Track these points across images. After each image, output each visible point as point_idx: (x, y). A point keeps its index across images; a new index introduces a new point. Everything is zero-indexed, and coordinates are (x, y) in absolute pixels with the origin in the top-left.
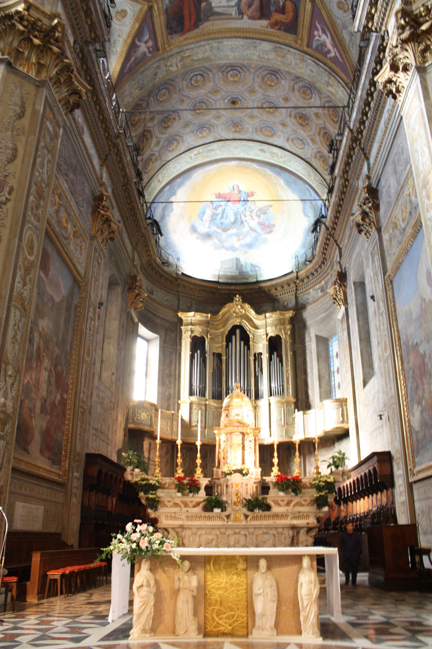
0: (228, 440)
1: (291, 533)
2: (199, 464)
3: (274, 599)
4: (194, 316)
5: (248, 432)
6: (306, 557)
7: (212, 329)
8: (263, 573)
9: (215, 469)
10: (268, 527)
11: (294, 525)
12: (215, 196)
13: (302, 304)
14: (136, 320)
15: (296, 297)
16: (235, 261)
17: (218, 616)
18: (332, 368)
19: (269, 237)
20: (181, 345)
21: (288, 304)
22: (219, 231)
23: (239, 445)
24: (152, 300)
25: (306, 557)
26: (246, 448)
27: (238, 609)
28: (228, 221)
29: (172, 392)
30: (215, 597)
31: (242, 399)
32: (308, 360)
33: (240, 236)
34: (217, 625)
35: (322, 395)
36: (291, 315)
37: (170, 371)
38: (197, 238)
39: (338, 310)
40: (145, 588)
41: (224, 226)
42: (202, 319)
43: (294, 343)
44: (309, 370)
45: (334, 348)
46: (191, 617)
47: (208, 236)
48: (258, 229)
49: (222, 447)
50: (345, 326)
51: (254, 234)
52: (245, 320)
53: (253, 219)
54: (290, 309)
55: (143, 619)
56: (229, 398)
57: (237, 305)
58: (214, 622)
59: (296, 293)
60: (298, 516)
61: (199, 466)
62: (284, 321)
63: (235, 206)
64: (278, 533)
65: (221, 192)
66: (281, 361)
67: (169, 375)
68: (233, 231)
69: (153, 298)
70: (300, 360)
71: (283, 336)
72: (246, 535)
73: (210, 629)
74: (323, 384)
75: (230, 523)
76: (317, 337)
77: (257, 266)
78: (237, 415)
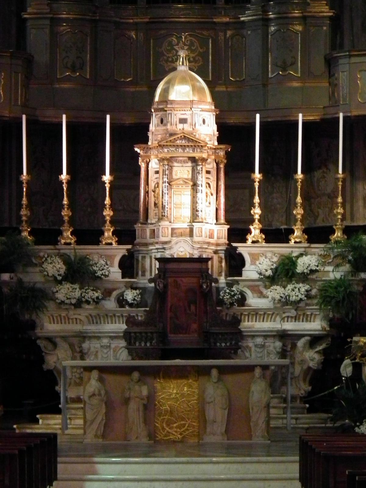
1: (278, 344)
3: (225, 407)
6: (258, 367)
8: (215, 383)
9: (138, 227)
11: (285, 331)
17: (168, 425)
25: (258, 367)
27: (189, 419)
30: (165, 408)
34: (167, 434)
40: (97, 397)
46: (142, 425)
49: (152, 185)
58: (164, 432)
61: (108, 222)
64: (256, 346)
73: (160, 437)
78: (183, 121)
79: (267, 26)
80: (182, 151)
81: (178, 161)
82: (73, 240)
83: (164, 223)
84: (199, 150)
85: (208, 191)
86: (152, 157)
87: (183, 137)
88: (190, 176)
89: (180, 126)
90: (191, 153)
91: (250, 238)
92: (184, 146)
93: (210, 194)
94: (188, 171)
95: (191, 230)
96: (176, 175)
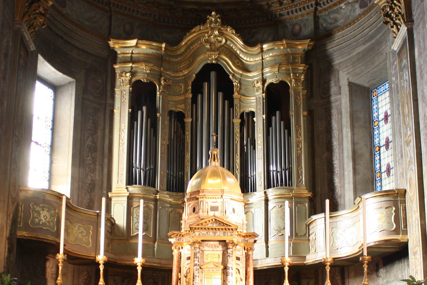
0: (195, 254)
4: (136, 46)
5: (235, 241)
7: (167, 70)
13: (325, 29)
14: (32, 47)
15: (316, 18)
18: (376, 141)
20: (113, 97)
21: (301, 29)
24: (63, 15)
26: (230, 271)
29: (97, 178)
31: (224, 179)
32: (335, 125)
35: (359, 187)
36: (306, 47)
37: (93, 142)
39: (391, 35)
42: (151, 51)
43: (309, 97)
44: (335, 143)
45: (380, 105)
49: (184, 271)
50: (406, 62)
52: (226, 55)
54: (305, 38)
56: (197, 178)
57: (213, 29)
59: (316, 9)
62: (294, 58)
66: (288, 127)
67: (93, 149)
69: (64, 12)
70: (320, 126)
71: (292, 84)
74: (361, 168)
76: (351, 85)
78: (215, 209)
80: (213, 235)
81: (209, 245)
84: (229, 234)
85: (238, 276)
86: (184, 244)
87: (214, 220)
88: (221, 260)
89: (211, 213)
90: (222, 236)
92: (215, 229)
93: (240, 280)
94: (219, 255)
96: (207, 259)
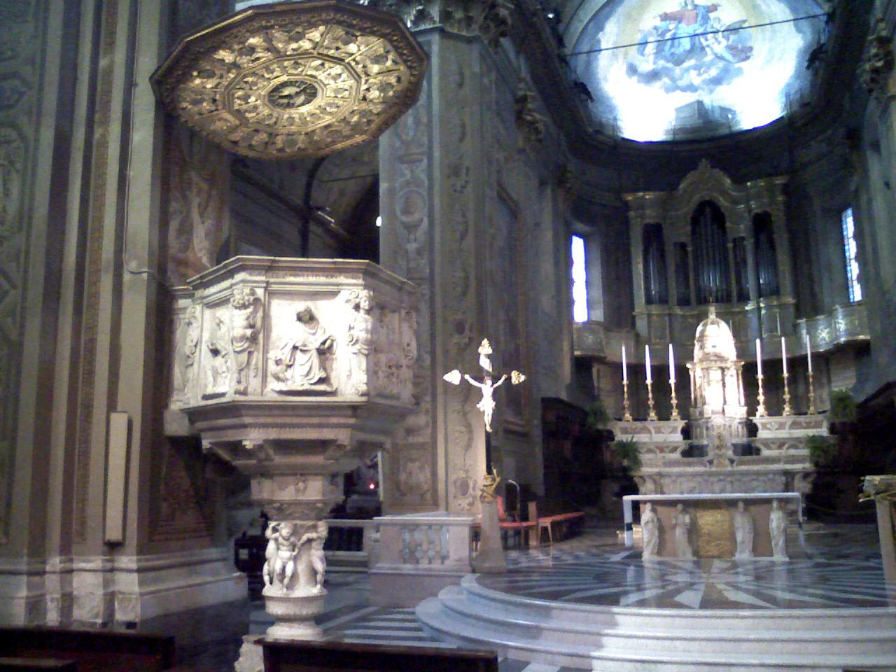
1: (783, 478)
2: (674, 405)
5: (729, 366)
9: (691, 410)
10: (758, 473)
12: (659, 19)
16: (696, 106)
19: (743, 65)
22: (670, 65)
23: (718, 382)
28: (682, 50)
33: (700, 69)
38: (639, 81)
40: (650, 524)
41: (676, 58)
43: (790, 219)
47: (654, 76)
48: (728, 56)
49: (698, 386)
51: (721, 64)
53: (719, 43)
55: (651, 546)
60: (793, 460)
63: (691, 27)
65: (668, 12)
68: (691, 62)
72: (732, 482)
75: (714, 469)
77: (729, 110)
78: (714, 347)
79: (760, 311)
82: (655, 418)
83: (705, 407)
91: (758, 414)
95: (723, 411)
